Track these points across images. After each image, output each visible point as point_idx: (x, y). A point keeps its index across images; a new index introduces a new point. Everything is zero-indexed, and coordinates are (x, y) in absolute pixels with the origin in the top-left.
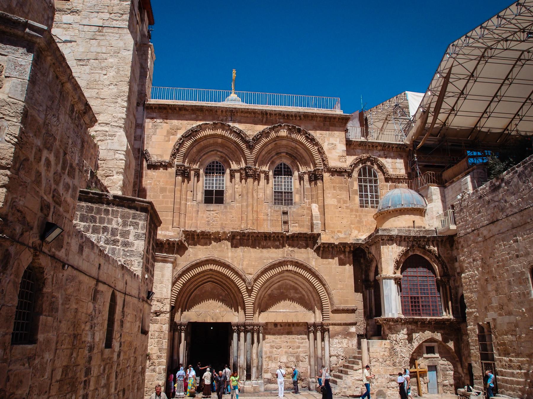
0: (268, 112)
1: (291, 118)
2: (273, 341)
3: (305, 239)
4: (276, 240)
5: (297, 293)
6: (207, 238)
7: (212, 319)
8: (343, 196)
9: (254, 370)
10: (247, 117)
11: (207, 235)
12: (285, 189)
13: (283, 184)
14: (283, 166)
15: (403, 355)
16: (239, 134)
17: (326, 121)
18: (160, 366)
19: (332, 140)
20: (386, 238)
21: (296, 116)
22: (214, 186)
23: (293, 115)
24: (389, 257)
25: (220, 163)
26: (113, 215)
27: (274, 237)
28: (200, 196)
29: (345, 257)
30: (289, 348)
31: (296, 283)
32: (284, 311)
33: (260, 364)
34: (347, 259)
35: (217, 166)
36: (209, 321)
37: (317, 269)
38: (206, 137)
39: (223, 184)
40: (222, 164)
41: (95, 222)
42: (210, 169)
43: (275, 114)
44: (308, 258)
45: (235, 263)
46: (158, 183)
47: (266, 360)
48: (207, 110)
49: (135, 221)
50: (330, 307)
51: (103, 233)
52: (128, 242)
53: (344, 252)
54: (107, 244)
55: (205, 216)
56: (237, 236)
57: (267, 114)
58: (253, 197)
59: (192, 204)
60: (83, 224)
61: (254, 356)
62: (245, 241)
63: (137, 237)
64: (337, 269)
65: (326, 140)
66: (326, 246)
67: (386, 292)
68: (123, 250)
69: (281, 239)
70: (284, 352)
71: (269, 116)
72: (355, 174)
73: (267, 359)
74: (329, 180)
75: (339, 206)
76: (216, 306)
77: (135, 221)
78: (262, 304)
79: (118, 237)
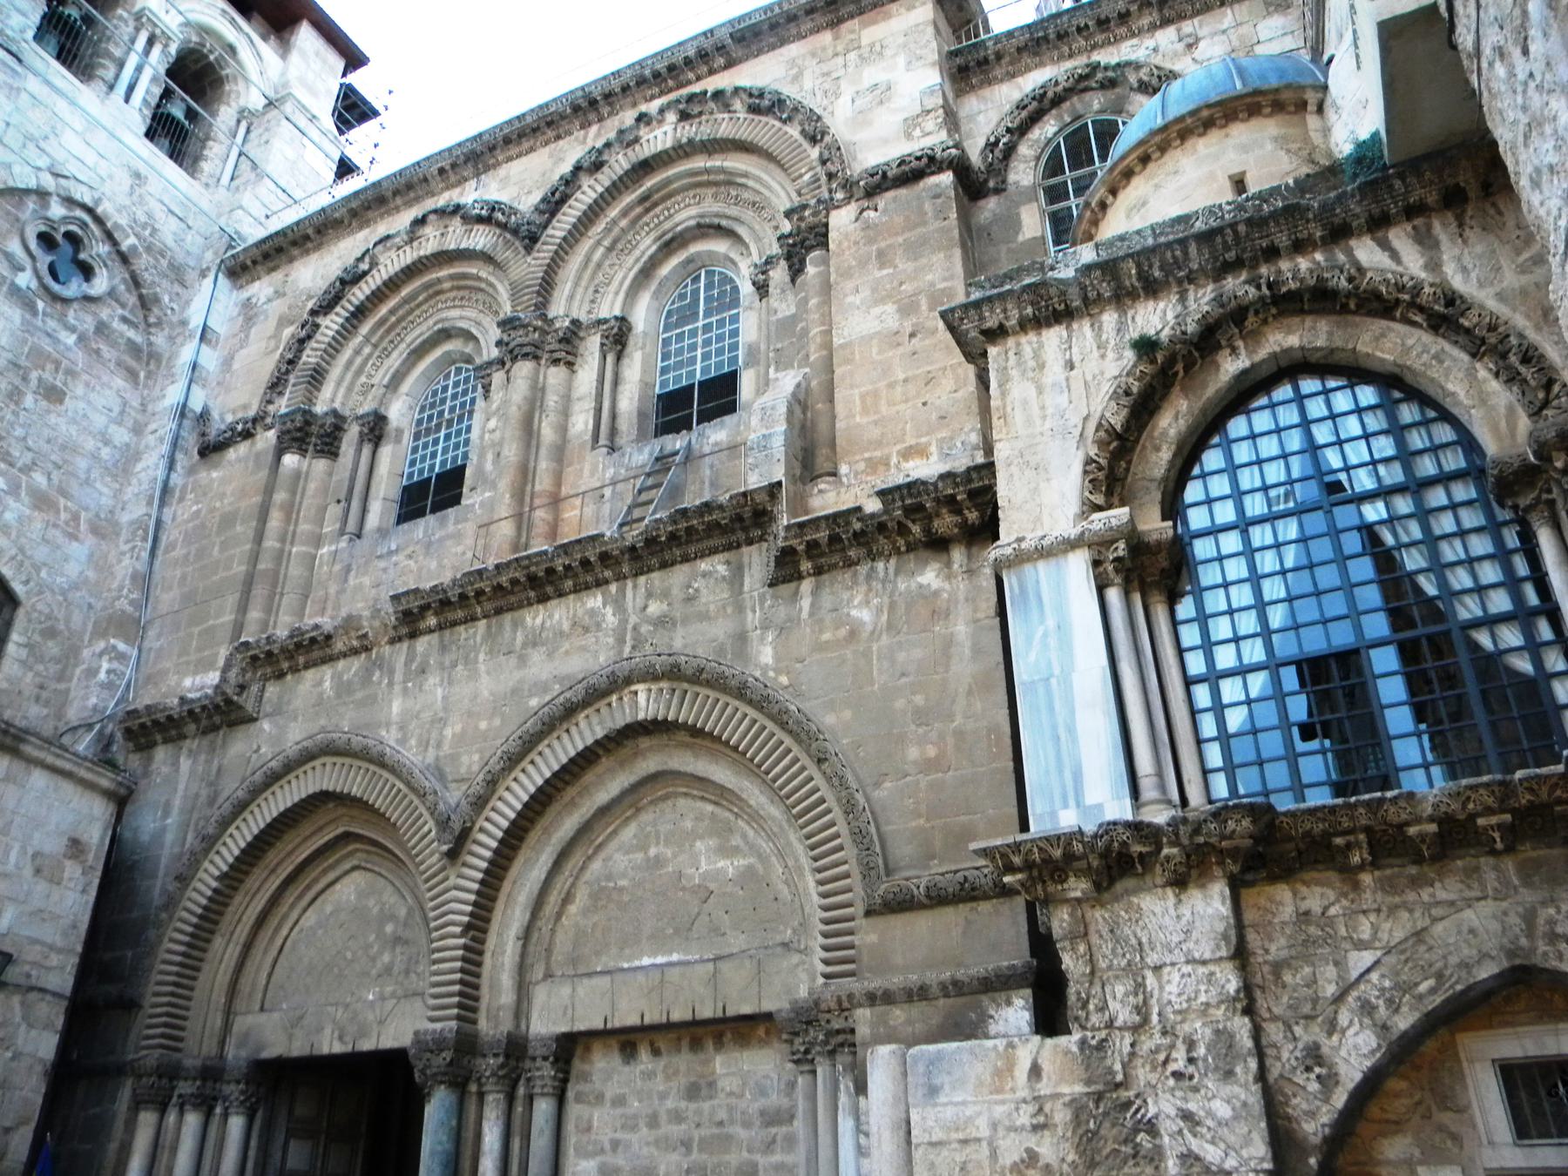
0: (597, 94)
1: (691, 75)
2: (615, 1144)
4: (587, 587)
7: (341, 1038)
8: (929, 277)
10: (532, 150)
11: (313, 640)
12: (705, 370)
13: (699, 352)
14: (702, 285)
15: (1212, 1154)
16: (489, 216)
17: (841, 21)
19: (873, 74)
20: (1014, 314)
21: (703, 55)
23: (691, 53)
24: (1048, 425)
27: (568, 568)
28: (378, 513)
29: (949, 577)
32: (660, 960)
34: (962, 585)
35: (456, 384)
36: (326, 1048)
37: (784, 680)
38: (392, 284)
39: (467, 442)
42: (433, 406)
43: (625, 89)
44: (741, 638)
45: (413, 742)
46: (218, 504)
48: (396, 193)
50: (859, 890)
53: (938, 545)
55: (366, 581)
56: (424, 609)
57: (593, 103)
59: (333, 548)
62: (461, 628)
64: (901, 656)
65: (843, 84)
66: (822, 535)
67: (1032, 657)
69: (608, 574)
71: (605, 110)
72: (1024, 173)
74: (858, 235)
75: (909, 330)
76: (367, 974)
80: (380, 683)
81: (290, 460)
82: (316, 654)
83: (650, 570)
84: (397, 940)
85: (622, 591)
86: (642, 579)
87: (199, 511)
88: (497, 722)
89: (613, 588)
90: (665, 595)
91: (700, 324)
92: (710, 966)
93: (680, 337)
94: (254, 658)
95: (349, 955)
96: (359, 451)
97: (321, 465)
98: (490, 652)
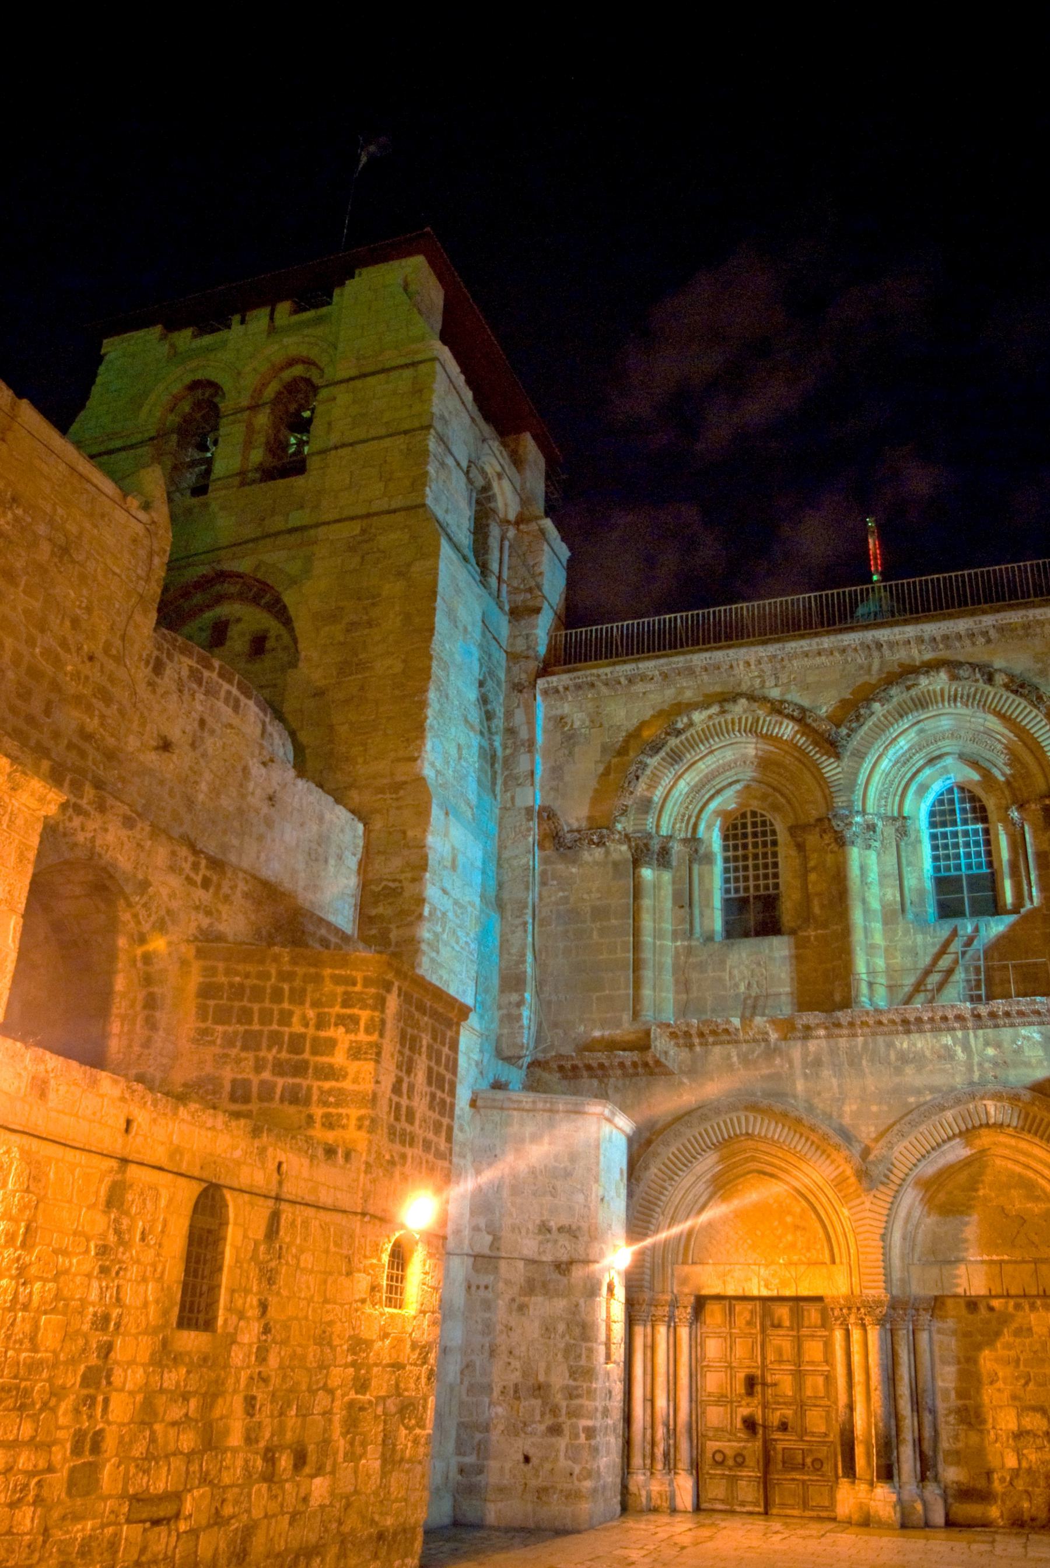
3: (1035, 1019)
4: (940, 1030)
5: (1037, 1199)
6: (729, 1042)
7: (766, 1286)
9: (907, 1454)
12: (969, 866)
18: (574, 1420)
22: (751, 883)
25: (762, 816)
26: (292, 1001)
30: (1023, 1381)
31: (1028, 1167)
32: (995, 1258)
33: (927, 1433)
35: (754, 825)
36: (755, 1293)
39: (776, 876)
40: (768, 816)
41: (250, 1022)
42: (735, 837)
46: (585, 896)
47: (947, 1423)
49: (348, 1011)
51: (269, 1048)
52: (331, 1066)
54: (282, 1074)
58: (864, 901)
60: (220, 1028)
61: (905, 1406)
63: (356, 1053)
68: (320, 1088)
69: (957, 1025)
70: (1006, 1395)
73: (952, 1419)
77: (348, 1011)
78: (920, 1237)
79: (306, 1055)
80: (782, 1067)
81: (647, 873)
82: (726, 1037)
83: (986, 1027)
84: (797, 1227)
85: (966, 1037)
86: (980, 1032)
87: (567, 898)
88: (885, 1108)
89: (959, 1034)
90: (998, 1045)
91: (959, 828)
92: (1033, 1266)
93: (944, 835)
94: (671, 1033)
95: (759, 1233)
96: (690, 869)
97: (667, 876)
98: (872, 1061)
